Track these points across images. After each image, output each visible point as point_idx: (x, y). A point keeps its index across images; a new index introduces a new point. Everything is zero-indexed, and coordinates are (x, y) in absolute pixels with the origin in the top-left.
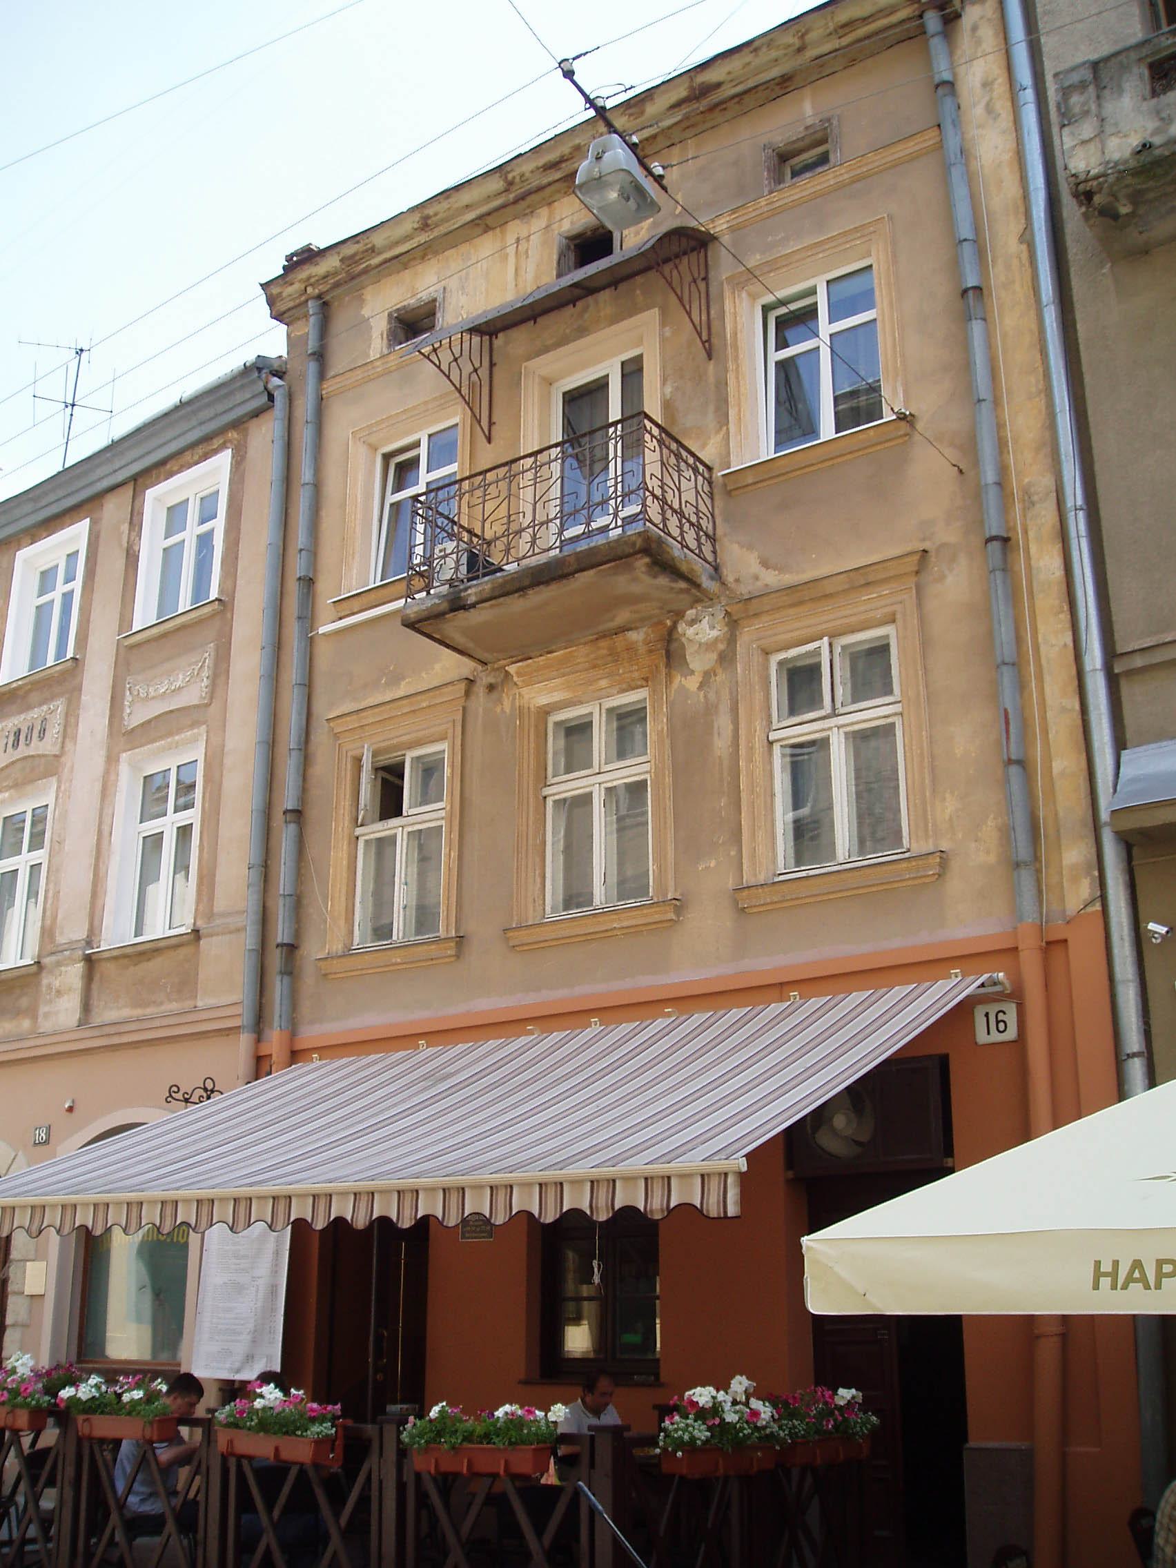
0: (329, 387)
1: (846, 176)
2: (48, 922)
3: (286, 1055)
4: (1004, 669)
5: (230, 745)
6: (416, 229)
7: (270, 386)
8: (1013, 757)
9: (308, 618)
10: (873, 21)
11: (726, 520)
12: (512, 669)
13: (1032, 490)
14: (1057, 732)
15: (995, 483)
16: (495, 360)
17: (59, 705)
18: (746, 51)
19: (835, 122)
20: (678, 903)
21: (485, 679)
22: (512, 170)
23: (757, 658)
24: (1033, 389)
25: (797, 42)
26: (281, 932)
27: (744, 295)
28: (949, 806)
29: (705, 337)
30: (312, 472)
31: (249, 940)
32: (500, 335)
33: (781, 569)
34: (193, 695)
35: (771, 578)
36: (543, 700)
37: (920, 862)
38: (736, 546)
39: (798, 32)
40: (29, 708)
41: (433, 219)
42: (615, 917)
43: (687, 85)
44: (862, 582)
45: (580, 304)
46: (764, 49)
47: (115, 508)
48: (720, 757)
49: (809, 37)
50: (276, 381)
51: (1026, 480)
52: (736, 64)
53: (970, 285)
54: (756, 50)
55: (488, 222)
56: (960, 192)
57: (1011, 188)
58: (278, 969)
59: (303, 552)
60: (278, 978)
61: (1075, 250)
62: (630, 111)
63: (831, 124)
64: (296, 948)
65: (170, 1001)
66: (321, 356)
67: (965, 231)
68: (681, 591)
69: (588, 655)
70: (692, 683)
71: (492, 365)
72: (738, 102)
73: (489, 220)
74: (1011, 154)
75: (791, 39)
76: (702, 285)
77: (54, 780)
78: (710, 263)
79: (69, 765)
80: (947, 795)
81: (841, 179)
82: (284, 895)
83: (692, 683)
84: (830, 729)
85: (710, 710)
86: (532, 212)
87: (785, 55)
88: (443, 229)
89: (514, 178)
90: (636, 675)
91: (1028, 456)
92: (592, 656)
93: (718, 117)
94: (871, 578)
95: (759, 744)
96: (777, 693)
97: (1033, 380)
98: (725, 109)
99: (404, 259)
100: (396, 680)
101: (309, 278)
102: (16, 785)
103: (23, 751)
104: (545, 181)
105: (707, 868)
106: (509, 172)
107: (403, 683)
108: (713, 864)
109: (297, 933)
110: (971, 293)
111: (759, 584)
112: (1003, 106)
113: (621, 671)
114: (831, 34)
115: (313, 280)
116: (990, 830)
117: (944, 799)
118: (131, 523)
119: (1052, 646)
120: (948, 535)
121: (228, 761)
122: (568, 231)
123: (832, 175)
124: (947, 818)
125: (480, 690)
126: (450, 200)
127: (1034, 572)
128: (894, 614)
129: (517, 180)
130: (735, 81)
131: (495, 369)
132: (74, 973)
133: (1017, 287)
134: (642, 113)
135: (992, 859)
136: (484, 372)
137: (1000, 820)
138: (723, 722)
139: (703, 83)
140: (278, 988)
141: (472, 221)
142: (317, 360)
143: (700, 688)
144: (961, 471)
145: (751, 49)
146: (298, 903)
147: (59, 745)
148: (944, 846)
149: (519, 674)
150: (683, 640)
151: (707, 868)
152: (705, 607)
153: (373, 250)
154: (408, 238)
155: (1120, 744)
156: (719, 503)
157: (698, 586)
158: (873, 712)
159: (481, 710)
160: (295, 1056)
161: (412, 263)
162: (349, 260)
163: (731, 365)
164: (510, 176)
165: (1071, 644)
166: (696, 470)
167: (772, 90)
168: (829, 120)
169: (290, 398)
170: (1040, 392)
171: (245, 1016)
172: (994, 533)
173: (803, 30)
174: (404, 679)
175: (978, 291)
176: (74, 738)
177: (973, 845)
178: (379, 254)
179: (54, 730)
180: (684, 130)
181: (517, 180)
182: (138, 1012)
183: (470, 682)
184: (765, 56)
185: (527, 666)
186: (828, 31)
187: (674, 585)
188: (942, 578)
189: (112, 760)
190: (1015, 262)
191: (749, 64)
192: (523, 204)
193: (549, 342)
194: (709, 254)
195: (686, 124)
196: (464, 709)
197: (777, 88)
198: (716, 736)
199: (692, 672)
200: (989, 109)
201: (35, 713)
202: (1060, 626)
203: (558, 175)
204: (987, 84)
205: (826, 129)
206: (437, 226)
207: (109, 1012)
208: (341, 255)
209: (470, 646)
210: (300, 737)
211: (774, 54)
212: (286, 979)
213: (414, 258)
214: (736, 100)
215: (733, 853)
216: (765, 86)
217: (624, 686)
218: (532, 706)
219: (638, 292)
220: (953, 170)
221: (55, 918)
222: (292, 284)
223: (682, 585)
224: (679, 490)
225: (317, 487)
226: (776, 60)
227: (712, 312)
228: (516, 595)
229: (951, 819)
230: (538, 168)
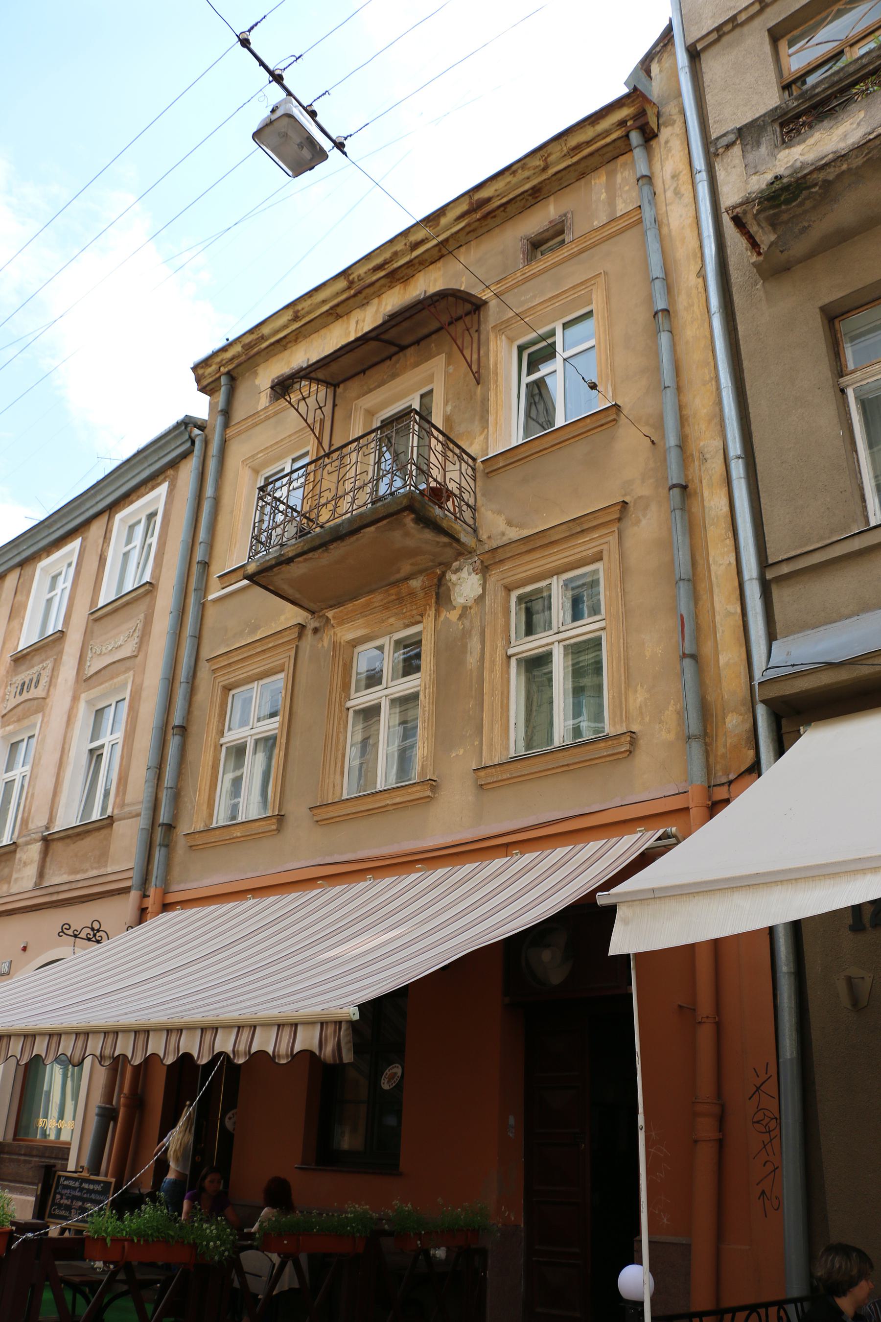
0: (230, 432)
1: (576, 249)
2: (26, 815)
3: (158, 906)
4: (681, 584)
5: (145, 684)
6: (290, 321)
7: (193, 435)
8: (687, 652)
9: (203, 589)
10: (596, 143)
11: (483, 495)
12: (330, 614)
13: (706, 450)
14: (723, 632)
15: (677, 446)
16: (337, 402)
17: (49, 663)
18: (507, 173)
19: (569, 216)
20: (434, 783)
21: (313, 624)
22: (352, 273)
23: (502, 593)
24: (707, 378)
25: (541, 163)
26: (163, 817)
27: (504, 337)
28: (638, 698)
29: (475, 369)
30: (213, 489)
31: (142, 822)
32: (342, 386)
33: (520, 526)
34: (126, 652)
35: (514, 534)
36: (350, 636)
37: (615, 742)
38: (490, 513)
39: (542, 157)
40: (33, 667)
41: (301, 312)
42: (387, 795)
43: (468, 202)
44: (579, 530)
45: (394, 359)
46: (520, 171)
47: (96, 529)
48: (471, 670)
49: (551, 159)
50: (196, 431)
51: (702, 444)
52: (500, 185)
53: (659, 308)
54: (514, 172)
55: (337, 312)
56: (653, 247)
57: (693, 243)
58: (158, 843)
59: (202, 544)
60: (158, 849)
61: (736, 276)
62: (430, 224)
63: (567, 218)
64: (174, 828)
65: (92, 868)
66: (227, 413)
67: (656, 271)
68: (445, 545)
69: (382, 600)
70: (453, 616)
71: (334, 405)
72: (504, 211)
73: (339, 310)
74: (691, 219)
75: (537, 162)
76: (475, 336)
77: (40, 715)
78: (482, 319)
79: (50, 703)
80: (639, 687)
81: (572, 251)
82: (167, 788)
83: (453, 616)
84: (553, 643)
85: (466, 634)
86: (368, 303)
87: (534, 174)
88: (307, 319)
89: (354, 278)
91: (703, 426)
92: (385, 601)
93: (491, 222)
94: (585, 526)
95: (499, 659)
96: (517, 618)
97: (706, 371)
98: (495, 217)
99: (284, 342)
100: (255, 628)
101: (222, 360)
102: (19, 720)
103: (26, 696)
104: (374, 278)
105: (457, 755)
106: (350, 275)
107: (259, 632)
108: (461, 752)
109: (175, 815)
110: (660, 314)
112: (686, 189)
113: (404, 611)
114: (565, 155)
115: (224, 362)
116: (670, 714)
117: (636, 691)
118: (105, 538)
119: (720, 565)
120: (643, 490)
121: (144, 694)
122: (390, 311)
123: (566, 250)
124: (638, 705)
125: (309, 632)
126: (312, 298)
127: (706, 510)
128: (601, 552)
129: (356, 280)
130: (500, 196)
131: (336, 409)
132: (35, 849)
133: (696, 308)
134: (438, 224)
135: (671, 737)
136: (328, 410)
138: (474, 644)
139: (477, 200)
140: (158, 855)
141: (327, 311)
142: (224, 415)
143: (461, 617)
144: (653, 442)
145: (510, 172)
146: (177, 796)
147: (46, 691)
148: (634, 728)
150: (449, 584)
151: (457, 755)
152: (466, 559)
153: (263, 338)
154: (285, 327)
155: (771, 636)
156: (479, 483)
157: (458, 541)
158: (587, 628)
159: (308, 647)
160: (166, 907)
161: (289, 345)
162: (248, 347)
163: (492, 386)
164: (351, 278)
165: (734, 563)
166: (460, 458)
167: (527, 200)
168: (565, 215)
169: (206, 443)
170: (712, 379)
171: (133, 881)
172: (675, 482)
173: (546, 155)
174: (260, 628)
175: (666, 313)
176: (55, 686)
177: (657, 727)
178: (267, 340)
179: (44, 681)
180: (468, 233)
181: (356, 280)
182: (72, 878)
183: (302, 627)
184: (522, 175)
185: (341, 612)
186: (563, 154)
187: (438, 539)
188: (638, 522)
189: (75, 699)
190: (694, 292)
191: (510, 182)
192: (361, 296)
193: (372, 386)
194: (482, 313)
195: (468, 229)
196: (297, 646)
197: (530, 198)
198: (469, 653)
199: (454, 608)
200: (677, 193)
201: (36, 669)
203: (382, 273)
204: (675, 177)
205: (563, 221)
206: (304, 317)
207: (56, 877)
208: (242, 343)
209: (297, 596)
210: (188, 674)
211: (527, 174)
212: (163, 849)
213: (290, 342)
214: (502, 209)
215: (476, 743)
216: (521, 197)
217: (407, 622)
218: (342, 641)
219: (433, 345)
220: (648, 232)
221: (29, 813)
222: (211, 366)
223: (446, 540)
224: (444, 470)
225: (217, 501)
226: (528, 178)
227: (482, 352)
228: (320, 550)
229: (640, 707)
230: (369, 270)
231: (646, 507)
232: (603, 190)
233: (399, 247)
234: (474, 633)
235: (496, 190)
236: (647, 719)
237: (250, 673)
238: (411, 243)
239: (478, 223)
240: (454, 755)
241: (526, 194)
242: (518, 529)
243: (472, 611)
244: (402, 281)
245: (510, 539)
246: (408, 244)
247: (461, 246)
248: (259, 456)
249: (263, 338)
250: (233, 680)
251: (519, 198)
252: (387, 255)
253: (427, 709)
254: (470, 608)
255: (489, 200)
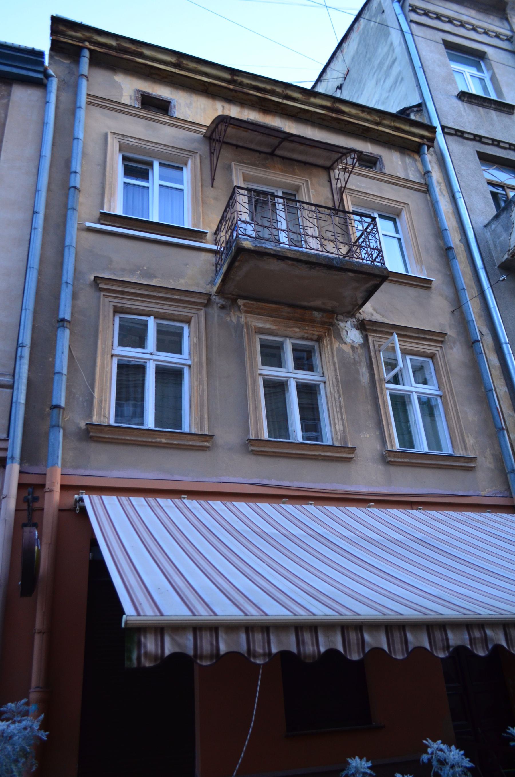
12: (240, 302)
14: (509, 423)
36: (260, 325)
52: (354, 111)
90: (316, 333)
98: (339, 123)
107: (155, 280)
108: (368, 436)
111: (373, 317)
115: (93, 40)
120: (451, 333)
124: (471, 444)
137: (492, 452)
149: (244, 305)
153: (141, 55)
164: (235, 78)
174: (155, 277)
177: (484, 459)
186: (391, 125)
188: (451, 348)
202: (502, 383)
203: (259, 94)
213: (159, 75)
214: (346, 123)
218: (252, 325)
229: (473, 445)
230: (251, 84)
231: (454, 343)
232: (399, 160)
233: (279, 90)
234: (362, 364)
235: (350, 111)
236: (478, 453)
237: (151, 309)
238: (287, 94)
239: (330, 118)
240: (362, 436)
241: (363, 127)
242: (381, 316)
243: (358, 350)
244: (263, 108)
245: (377, 320)
246: (285, 93)
247: (308, 120)
248: (130, 139)
249: (141, 55)
250: (129, 306)
251: (358, 126)
252: (269, 87)
253: (337, 399)
254: (357, 348)
255: (343, 113)
